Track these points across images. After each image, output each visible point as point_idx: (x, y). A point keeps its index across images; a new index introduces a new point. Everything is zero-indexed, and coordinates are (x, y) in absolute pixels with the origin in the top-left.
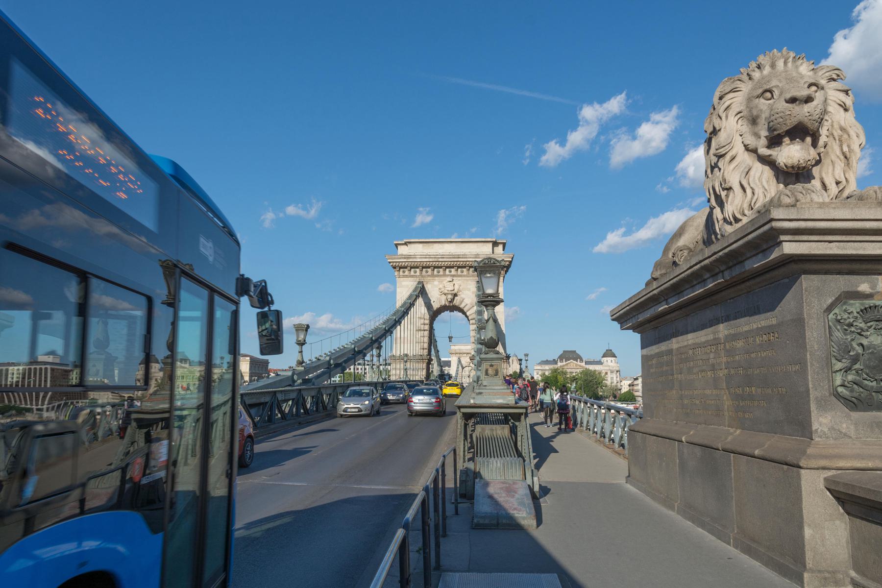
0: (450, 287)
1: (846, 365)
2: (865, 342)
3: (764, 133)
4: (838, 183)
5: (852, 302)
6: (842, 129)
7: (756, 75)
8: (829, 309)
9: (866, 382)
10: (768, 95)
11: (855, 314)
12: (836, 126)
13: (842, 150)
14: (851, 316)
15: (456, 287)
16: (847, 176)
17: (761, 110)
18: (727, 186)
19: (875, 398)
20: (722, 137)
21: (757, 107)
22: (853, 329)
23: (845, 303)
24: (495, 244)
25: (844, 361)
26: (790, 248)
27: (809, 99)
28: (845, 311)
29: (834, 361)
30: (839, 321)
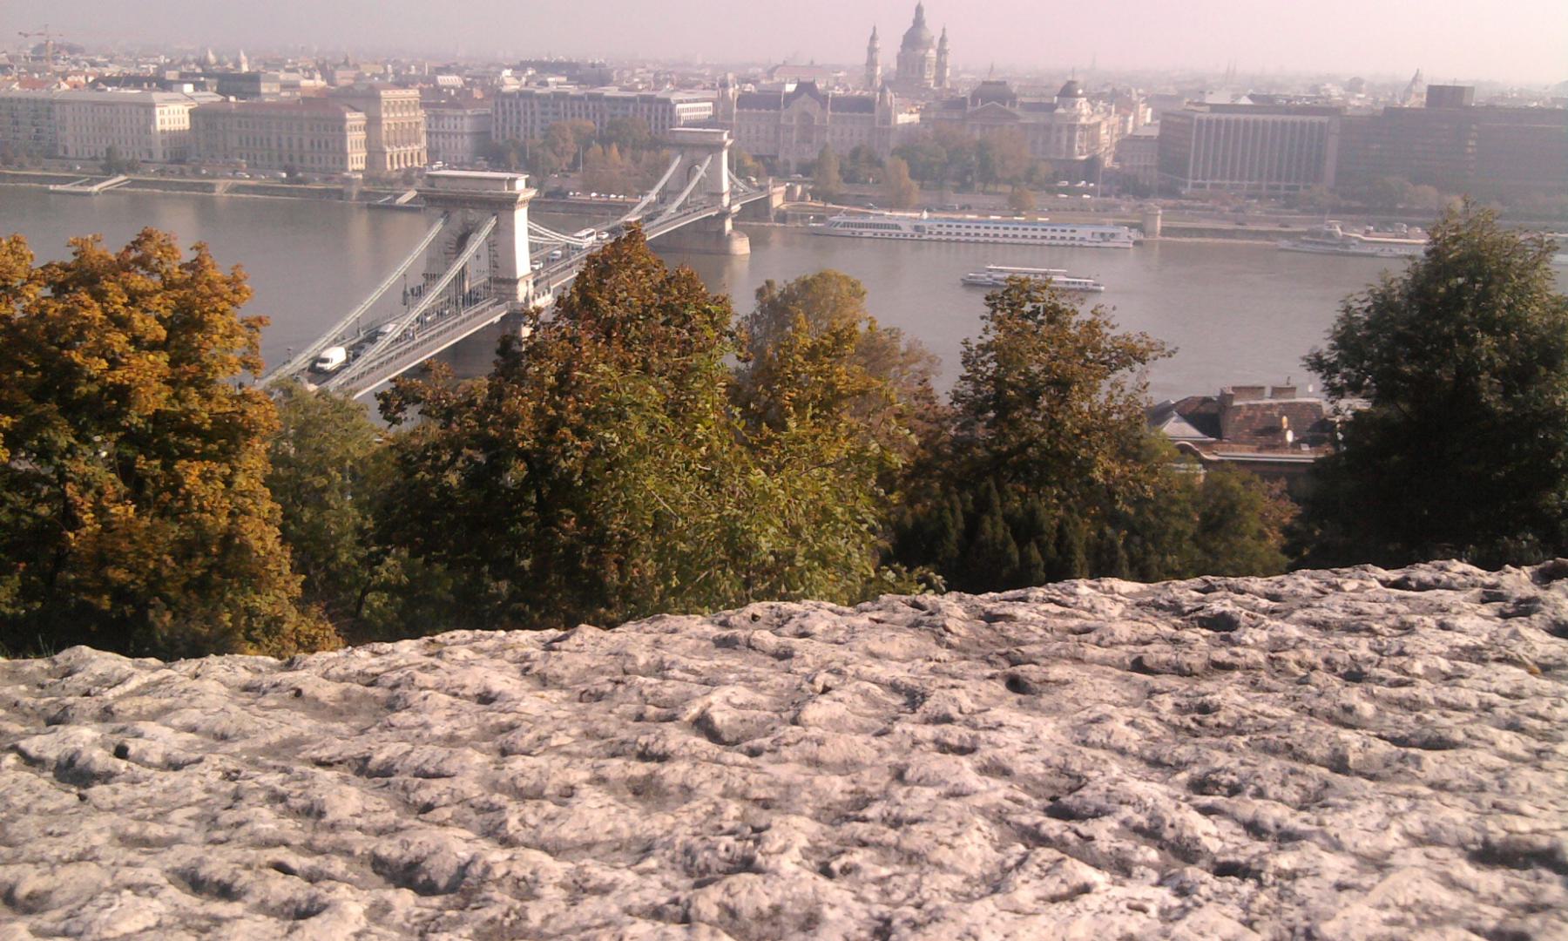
0: (470, 219)
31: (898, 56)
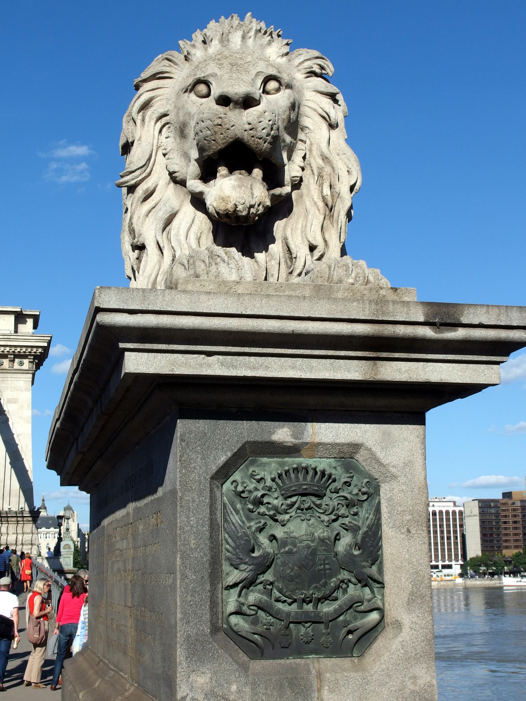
1: (244, 575)
2: (279, 532)
3: (195, 154)
4: (312, 248)
5: (265, 460)
6: (325, 158)
7: (198, 53)
8: (223, 473)
9: (280, 605)
10: (202, 88)
11: (269, 483)
12: (315, 152)
13: (322, 192)
14: (260, 486)
16: (327, 237)
17: (189, 114)
18: (139, 241)
19: (294, 633)
20: (137, 156)
21: (183, 107)
22: (262, 509)
23: (253, 463)
24: (20, 318)
25: (243, 567)
26: (137, 362)
27: (248, 102)
28: (252, 476)
29: (226, 567)
30: (239, 494)
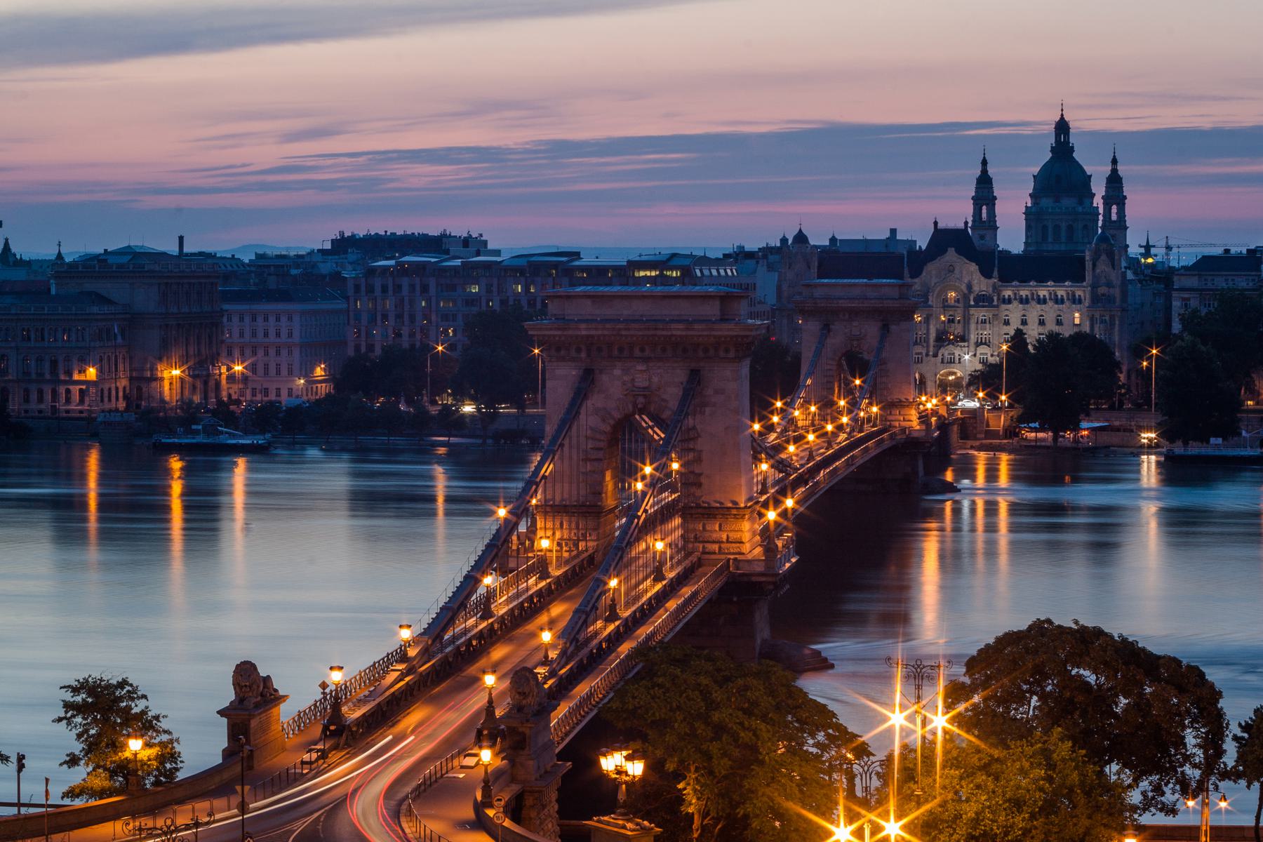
0: (641, 381)
15: (655, 379)
31: (1028, 212)
